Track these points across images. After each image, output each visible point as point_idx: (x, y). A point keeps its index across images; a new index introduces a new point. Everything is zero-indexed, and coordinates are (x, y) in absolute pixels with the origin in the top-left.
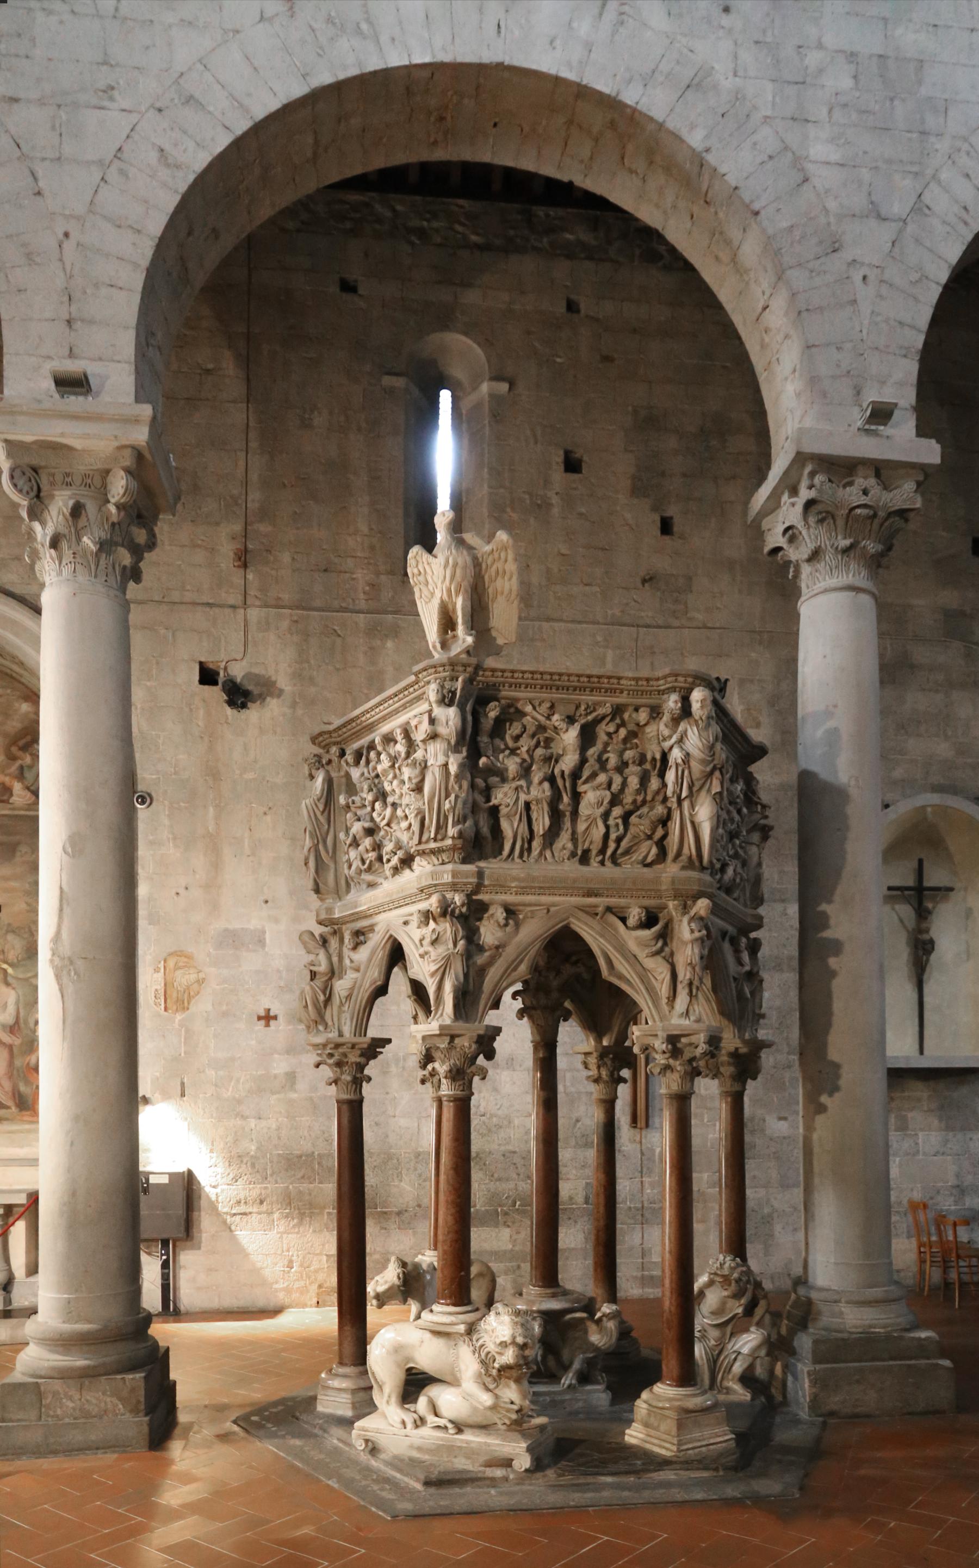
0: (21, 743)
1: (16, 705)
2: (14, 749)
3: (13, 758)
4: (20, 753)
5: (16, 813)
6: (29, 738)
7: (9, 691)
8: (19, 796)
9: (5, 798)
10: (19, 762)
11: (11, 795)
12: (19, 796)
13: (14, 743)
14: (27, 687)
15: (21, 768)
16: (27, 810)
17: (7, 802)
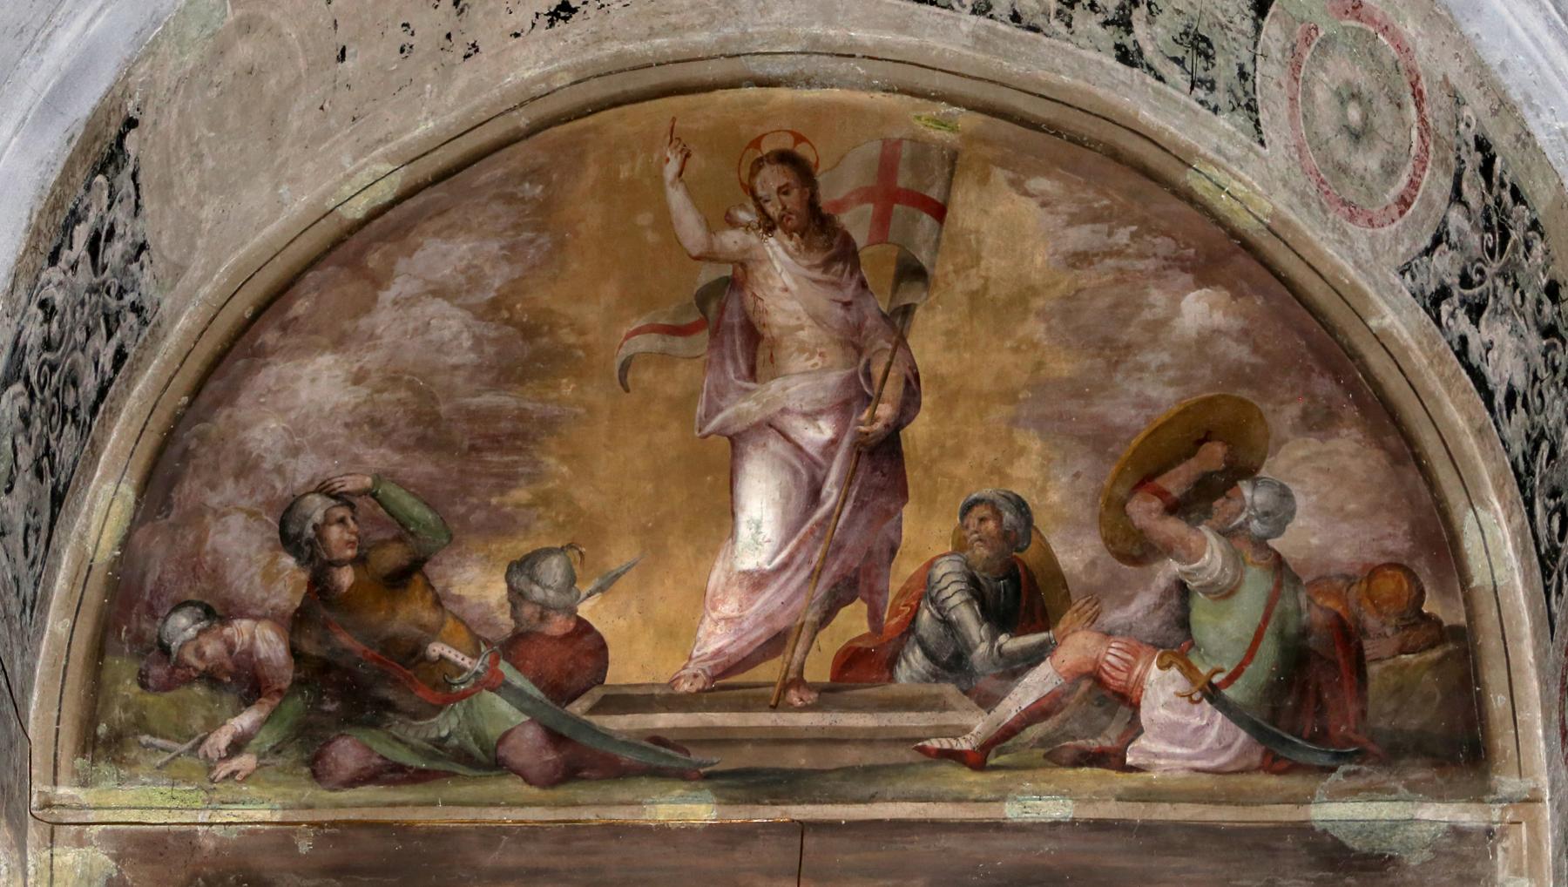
0: (1176, 482)
1: (1157, 297)
2: (1144, 511)
3: (1136, 550)
4: (1173, 527)
5: (1163, 812)
6: (1214, 455)
7: (1122, 236)
8: (1170, 732)
9: (1107, 741)
10: (1174, 567)
11: (1134, 729)
12: (1170, 732)
13: (1145, 473)
14: (1206, 210)
15: (1182, 589)
16: (1212, 799)
17: (1110, 759)
